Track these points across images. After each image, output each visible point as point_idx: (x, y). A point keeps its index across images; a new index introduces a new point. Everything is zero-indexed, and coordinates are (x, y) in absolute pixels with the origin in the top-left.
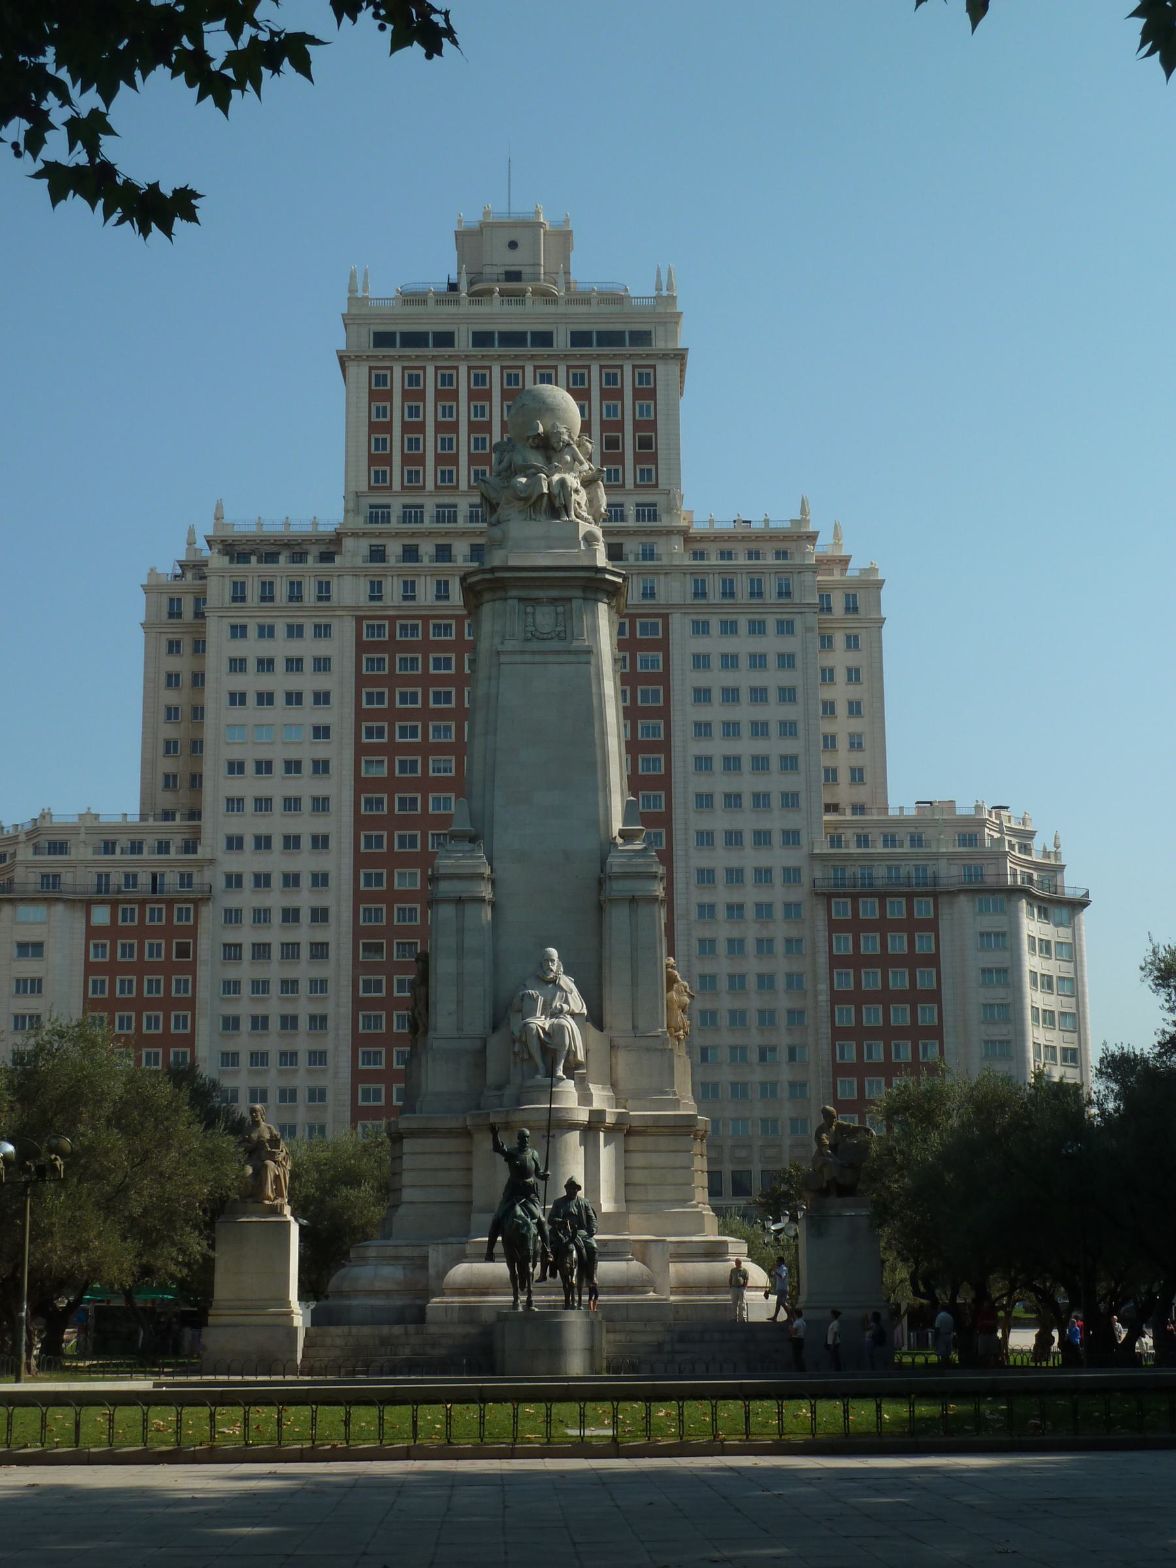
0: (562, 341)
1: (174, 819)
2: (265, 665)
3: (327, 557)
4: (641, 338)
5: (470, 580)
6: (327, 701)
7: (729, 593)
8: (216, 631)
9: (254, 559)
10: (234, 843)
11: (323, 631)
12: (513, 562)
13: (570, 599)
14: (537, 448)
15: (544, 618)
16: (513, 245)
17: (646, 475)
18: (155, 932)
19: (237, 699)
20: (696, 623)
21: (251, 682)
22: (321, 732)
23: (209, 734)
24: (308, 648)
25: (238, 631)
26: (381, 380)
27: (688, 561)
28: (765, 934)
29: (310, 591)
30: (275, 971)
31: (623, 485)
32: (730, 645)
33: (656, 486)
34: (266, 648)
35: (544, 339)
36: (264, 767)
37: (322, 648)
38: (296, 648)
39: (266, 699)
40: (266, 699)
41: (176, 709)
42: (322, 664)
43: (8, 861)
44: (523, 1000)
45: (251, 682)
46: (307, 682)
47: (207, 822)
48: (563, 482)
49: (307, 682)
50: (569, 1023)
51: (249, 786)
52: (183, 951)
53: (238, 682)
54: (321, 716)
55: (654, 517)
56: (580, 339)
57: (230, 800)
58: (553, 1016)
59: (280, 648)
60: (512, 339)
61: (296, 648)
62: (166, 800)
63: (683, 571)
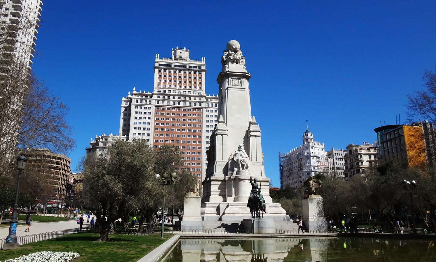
1: (125, 136)
2: (141, 113)
3: (151, 97)
4: (200, 67)
5: (222, 74)
6: (150, 119)
7: (212, 106)
8: (133, 107)
9: (139, 97)
11: (150, 108)
12: (229, 71)
13: (241, 79)
15: (237, 81)
16: (181, 53)
17: (200, 88)
19: (136, 118)
21: (138, 115)
22: (149, 123)
24: (147, 110)
25: (137, 107)
26: (160, 71)
27: (206, 101)
29: (148, 101)
34: (141, 110)
35: (185, 67)
36: (140, 128)
37: (150, 111)
38: (145, 111)
39: (140, 118)
40: (140, 118)
41: (126, 119)
42: (150, 113)
43: (98, 141)
44: (236, 154)
45: (138, 115)
46: (147, 116)
48: (239, 57)
49: (147, 116)
50: (245, 159)
53: (136, 115)
57: (134, 133)
58: (242, 157)
61: (145, 111)
63: (205, 102)
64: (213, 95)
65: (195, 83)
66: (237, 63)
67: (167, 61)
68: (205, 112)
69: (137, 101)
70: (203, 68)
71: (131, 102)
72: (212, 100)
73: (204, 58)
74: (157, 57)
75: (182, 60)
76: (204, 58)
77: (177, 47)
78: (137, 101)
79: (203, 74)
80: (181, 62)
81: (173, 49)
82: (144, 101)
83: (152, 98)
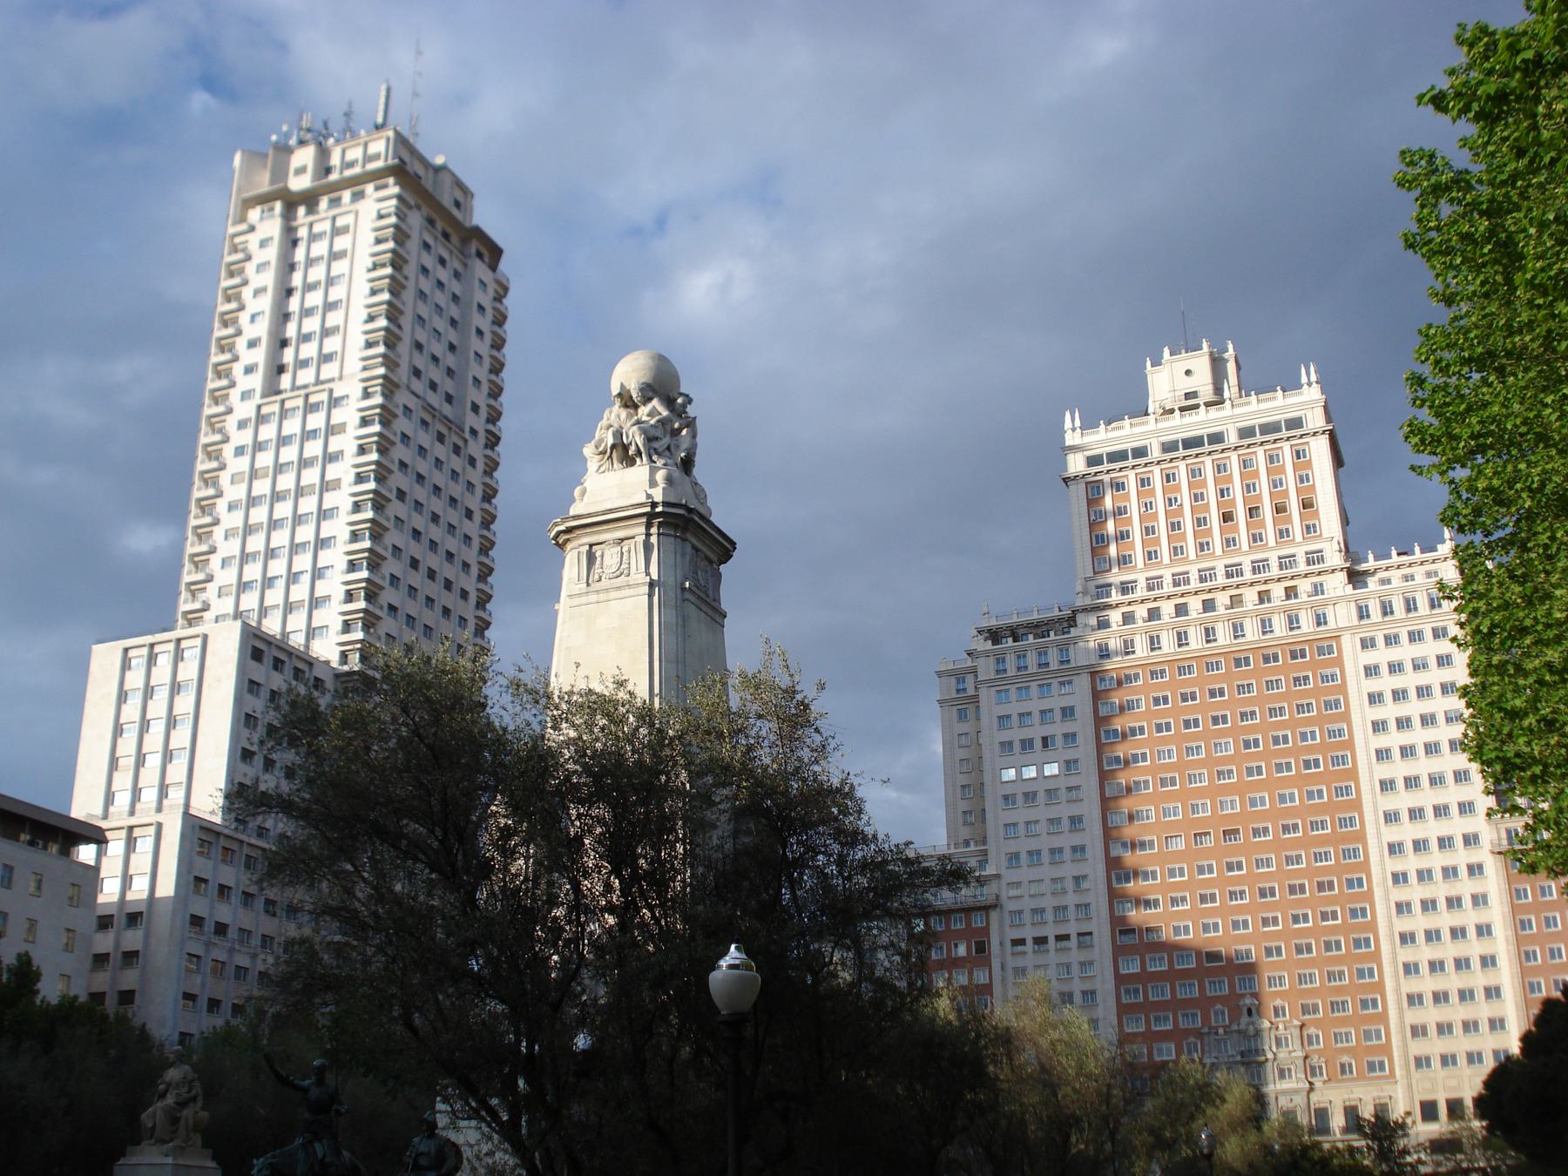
0: (1232, 438)
4: (1295, 423)
8: (987, 696)
10: (1014, 858)
13: (633, 538)
14: (626, 406)
16: (1188, 373)
18: (960, 935)
19: (1007, 746)
20: (1363, 641)
21: (1016, 735)
23: (987, 778)
28: (1453, 893)
29: (1053, 658)
30: (1052, 956)
31: (1294, 539)
32: (1394, 654)
33: (1321, 535)
35: (1216, 438)
39: (1027, 744)
40: (1027, 744)
47: (991, 847)
49: (1057, 729)
51: (1021, 815)
52: (982, 948)
53: (1005, 736)
54: (1070, 754)
55: (1321, 560)
56: (1246, 433)
59: (1035, 706)
60: (1189, 443)
62: (965, 833)
64: (1394, 553)
65: (1280, 509)
66: (630, 462)
67: (1125, 434)
68: (1353, 658)
69: (1000, 660)
70: (1316, 419)
71: (975, 673)
72: (1388, 581)
73: (1312, 369)
74: (1068, 424)
75: (1196, 407)
76: (1312, 369)
77: (1166, 351)
78: (1000, 660)
79: (1320, 450)
80: (1191, 418)
81: (1148, 363)
82: (1032, 660)
83: (1069, 632)
